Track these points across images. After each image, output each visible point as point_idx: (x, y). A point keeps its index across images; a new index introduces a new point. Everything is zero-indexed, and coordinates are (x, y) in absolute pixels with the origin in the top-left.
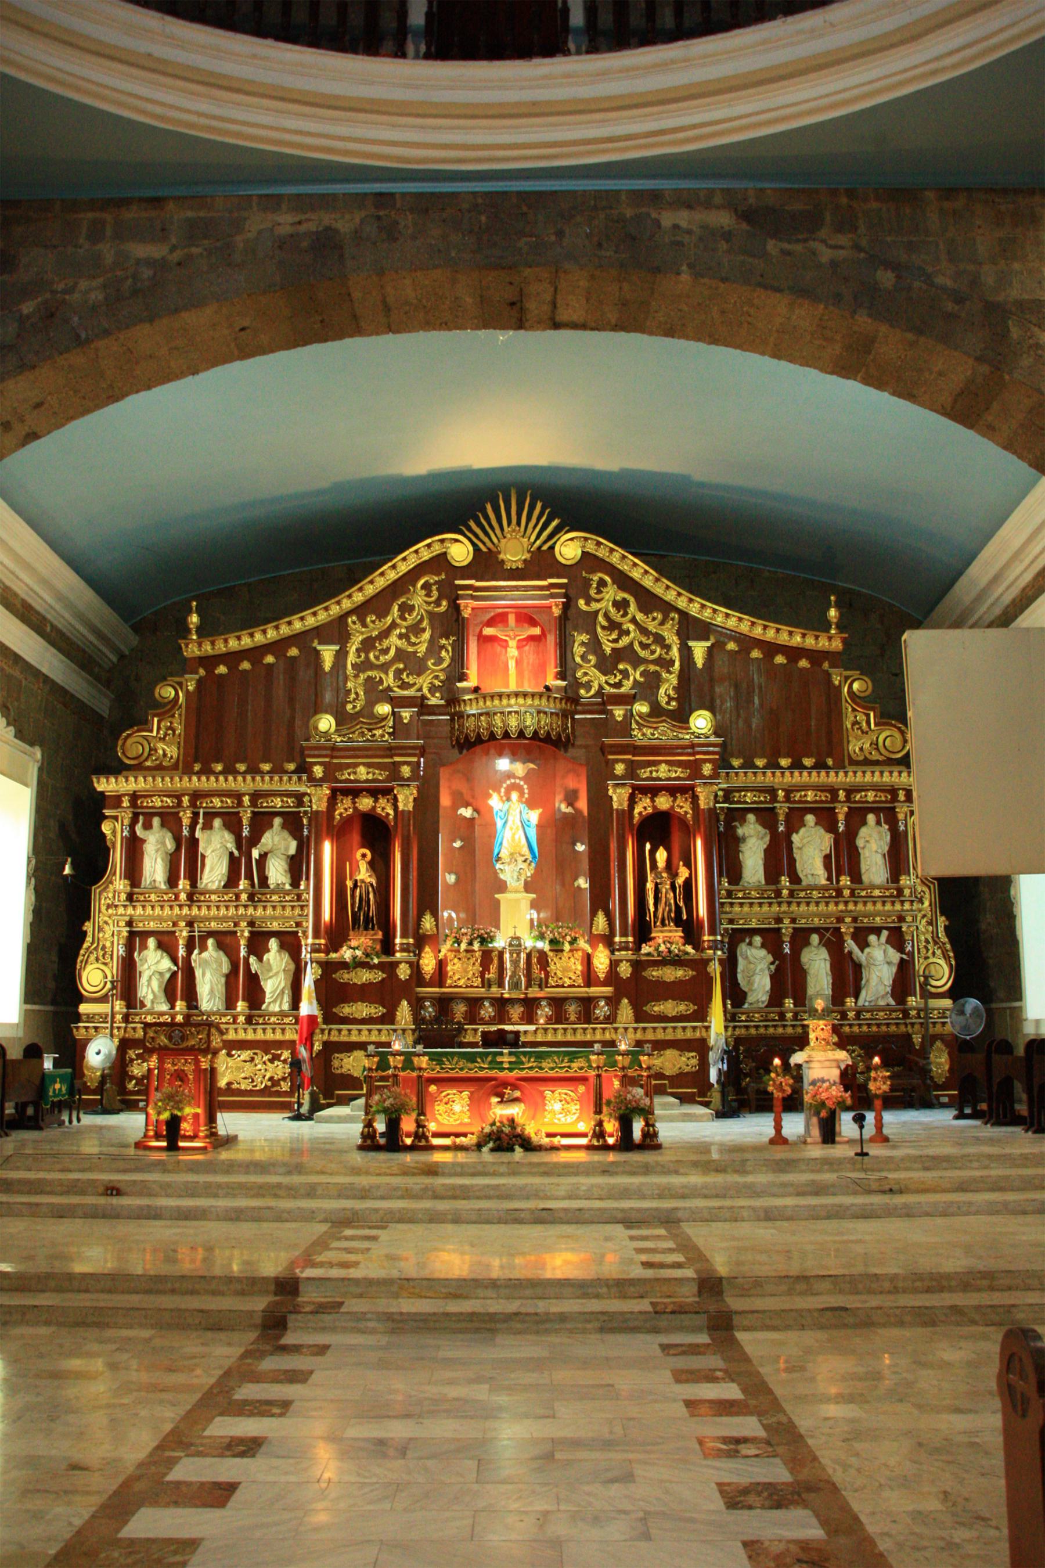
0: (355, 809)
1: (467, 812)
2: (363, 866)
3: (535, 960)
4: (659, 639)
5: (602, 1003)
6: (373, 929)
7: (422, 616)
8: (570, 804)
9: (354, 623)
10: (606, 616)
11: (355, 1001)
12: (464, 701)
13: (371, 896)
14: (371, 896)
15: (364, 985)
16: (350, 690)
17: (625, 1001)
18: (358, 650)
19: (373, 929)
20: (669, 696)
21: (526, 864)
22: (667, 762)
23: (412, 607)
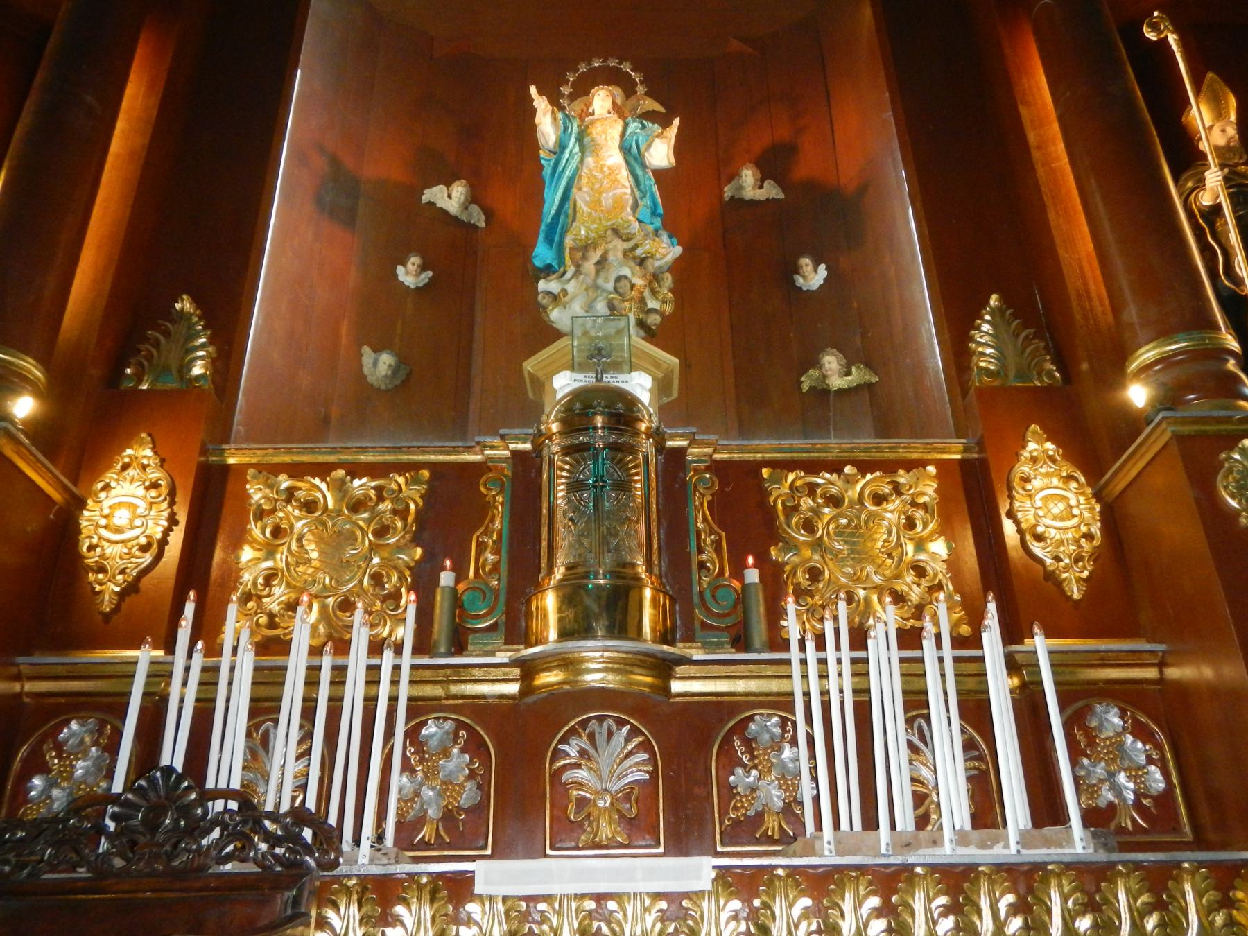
8: (766, 173)
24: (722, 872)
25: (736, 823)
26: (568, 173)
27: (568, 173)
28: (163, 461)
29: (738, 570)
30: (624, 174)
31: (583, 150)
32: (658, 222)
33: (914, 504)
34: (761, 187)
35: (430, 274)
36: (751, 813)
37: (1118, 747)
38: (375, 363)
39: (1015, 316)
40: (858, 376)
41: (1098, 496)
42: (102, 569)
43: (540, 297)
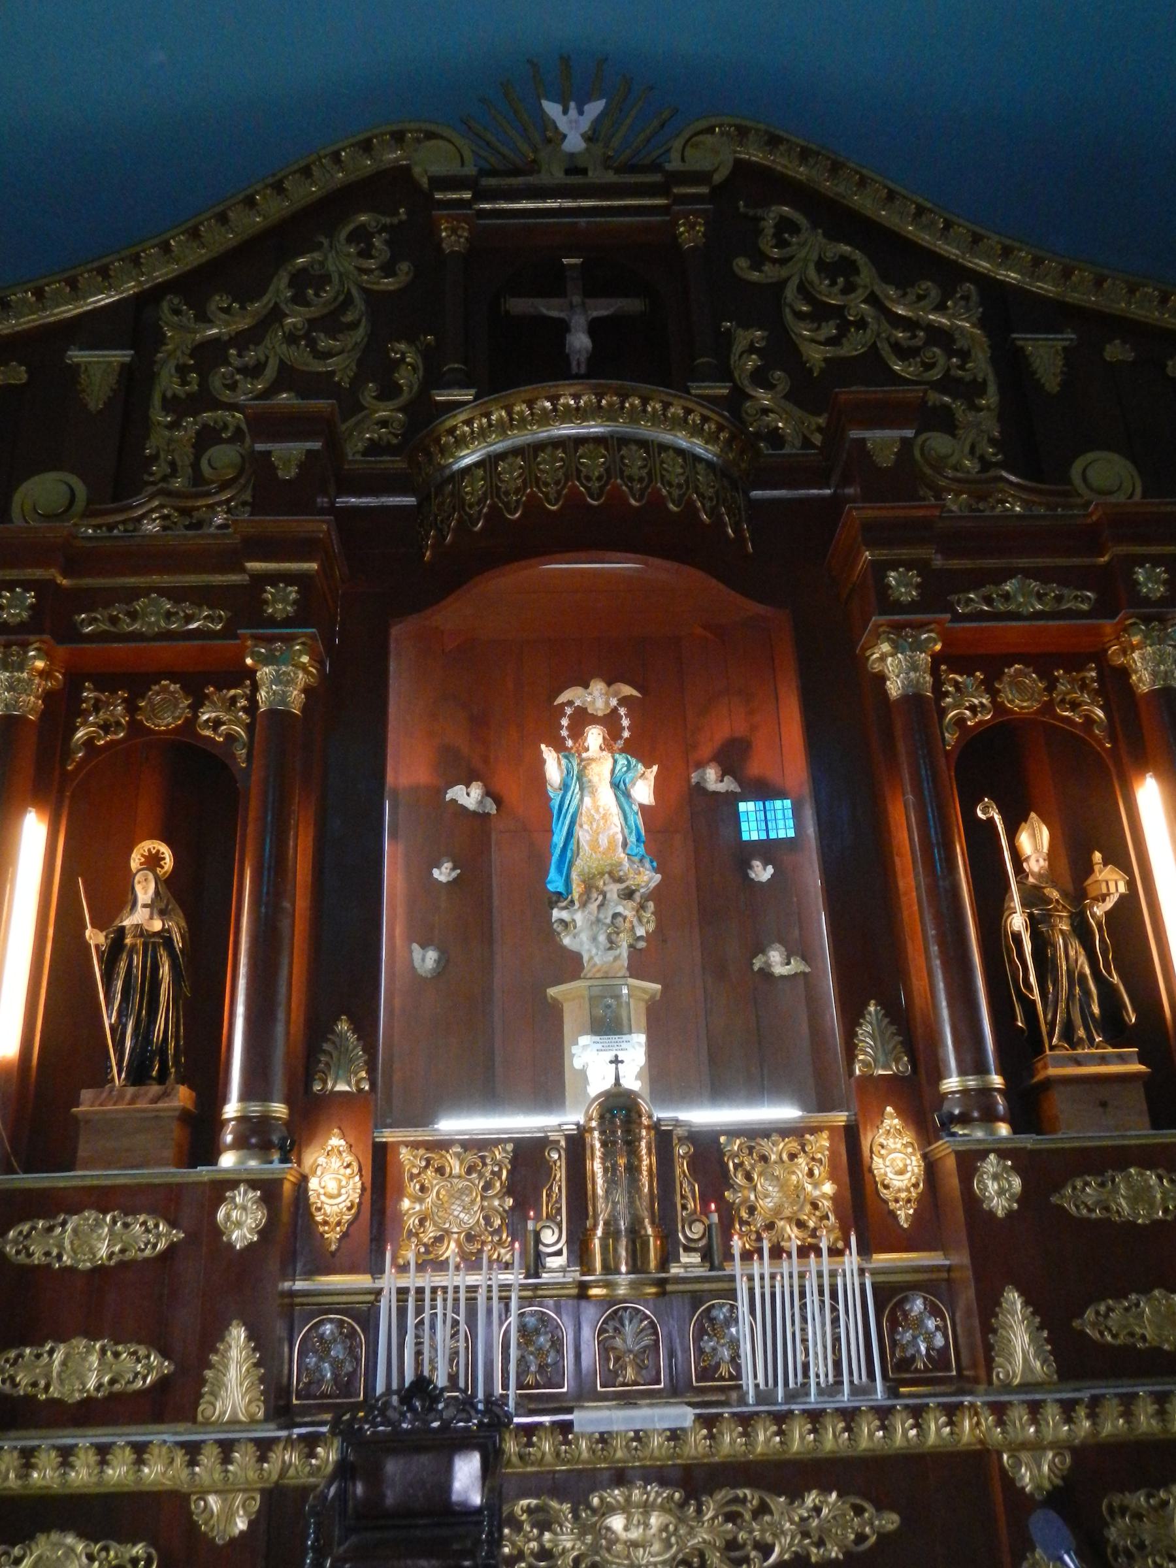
0: (135, 727)
1: (469, 796)
2: (145, 891)
3: (682, 1167)
4: (941, 337)
5: (918, 1305)
6: (162, 1078)
7: (349, 292)
8: (726, 771)
9: (177, 312)
10: (804, 291)
11: (62, 1338)
12: (451, 431)
13: (165, 971)
14: (165, 971)
15: (99, 1271)
16: (154, 458)
17: (1014, 1299)
18: (182, 370)
19: (162, 1078)
20: (982, 459)
21: (630, 904)
22: (1029, 573)
23: (325, 279)
24: (698, 1417)
25: (705, 1369)
26: (571, 810)
27: (571, 810)
28: (351, 1146)
29: (706, 1211)
30: (614, 809)
31: (582, 789)
32: (642, 850)
33: (813, 1159)
34: (722, 781)
35: (459, 871)
36: (713, 1363)
37: (919, 1323)
38: (423, 960)
39: (885, 1015)
40: (796, 966)
41: (925, 1157)
42: (326, 1223)
43: (555, 926)
